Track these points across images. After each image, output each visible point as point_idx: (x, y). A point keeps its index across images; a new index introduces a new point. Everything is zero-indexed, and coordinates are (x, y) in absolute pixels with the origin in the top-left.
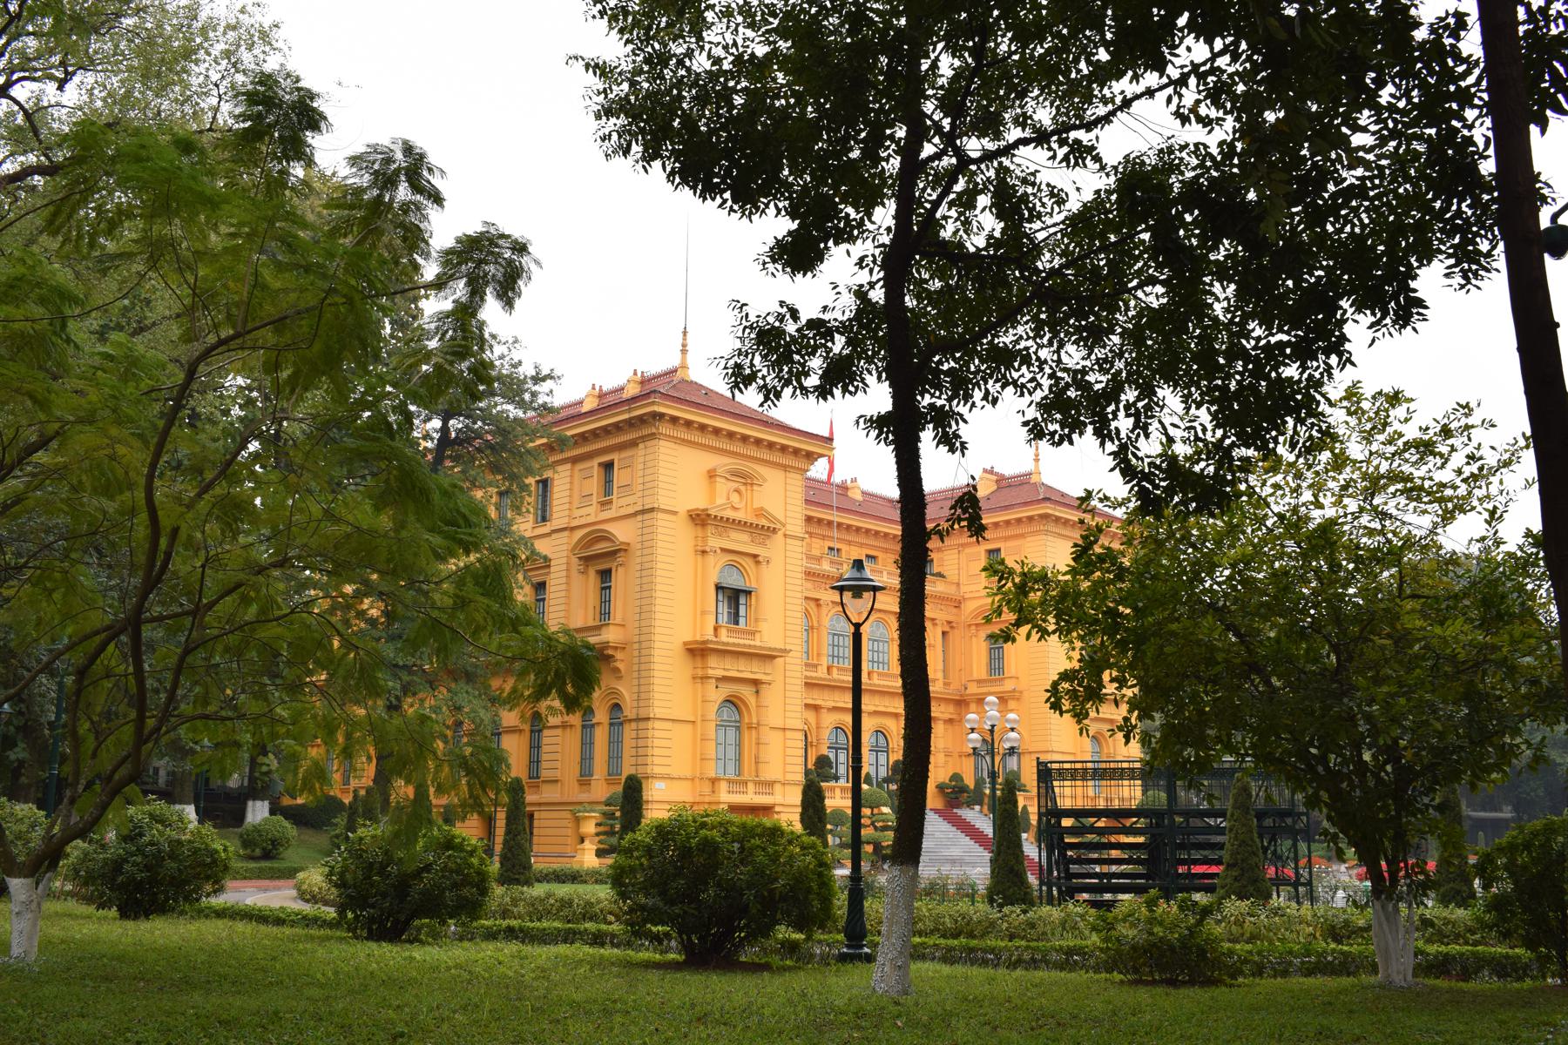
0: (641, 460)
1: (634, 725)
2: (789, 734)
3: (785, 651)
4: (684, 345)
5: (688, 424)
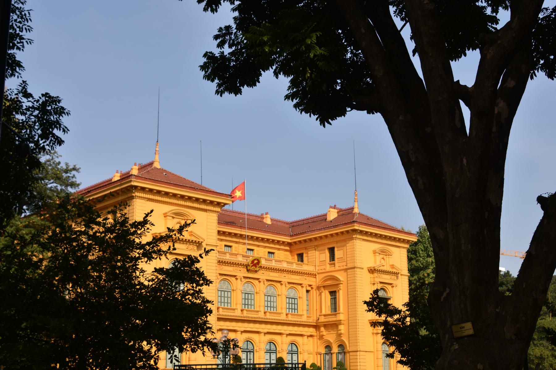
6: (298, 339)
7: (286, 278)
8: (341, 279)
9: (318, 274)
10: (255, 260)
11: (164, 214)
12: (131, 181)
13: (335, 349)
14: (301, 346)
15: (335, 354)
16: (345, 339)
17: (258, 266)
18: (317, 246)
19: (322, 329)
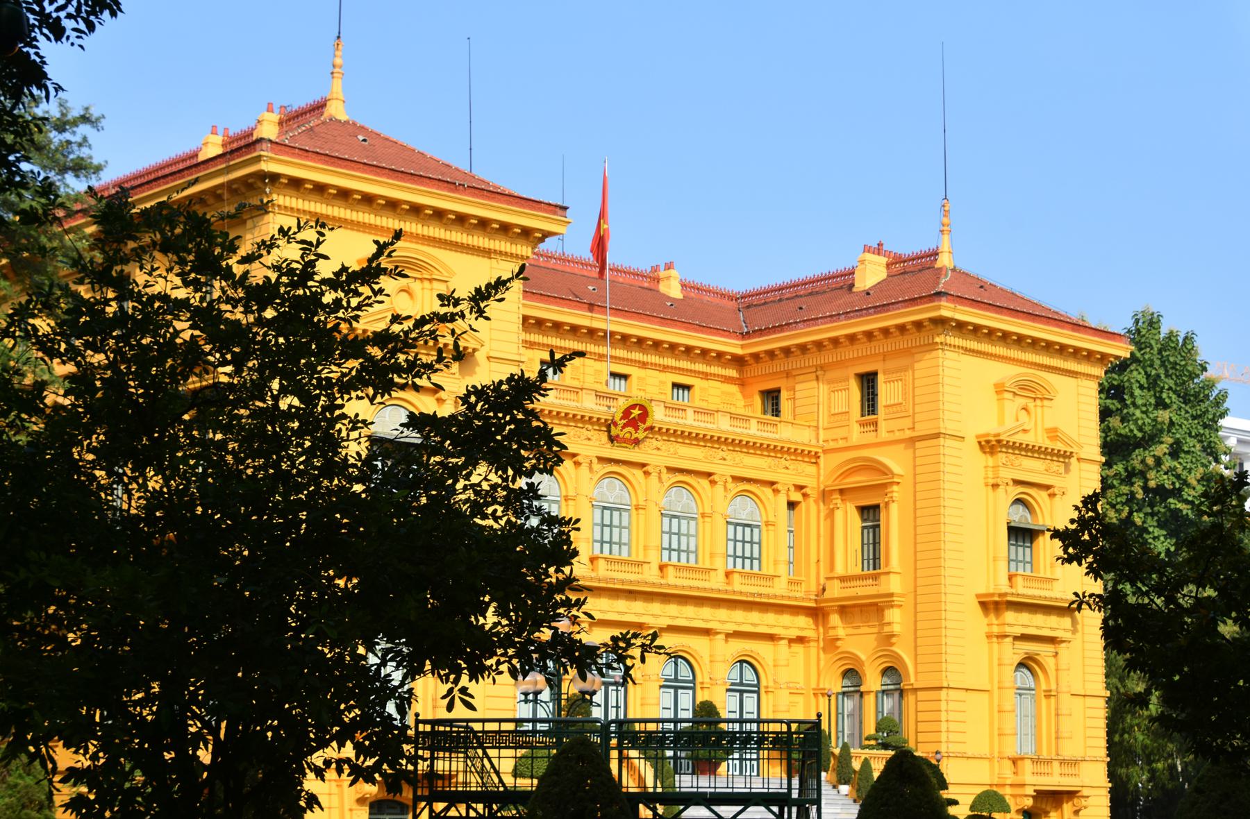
6: (762, 650)
7: (727, 464)
8: (896, 468)
9: (825, 452)
10: (633, 407)
12: (258, 159)
13: (873, 681)
14: (770, 670)
15: (872, 696)
16: (903, 651)
17: (642, 426)
18: (822, 367)
19: (835, 619)
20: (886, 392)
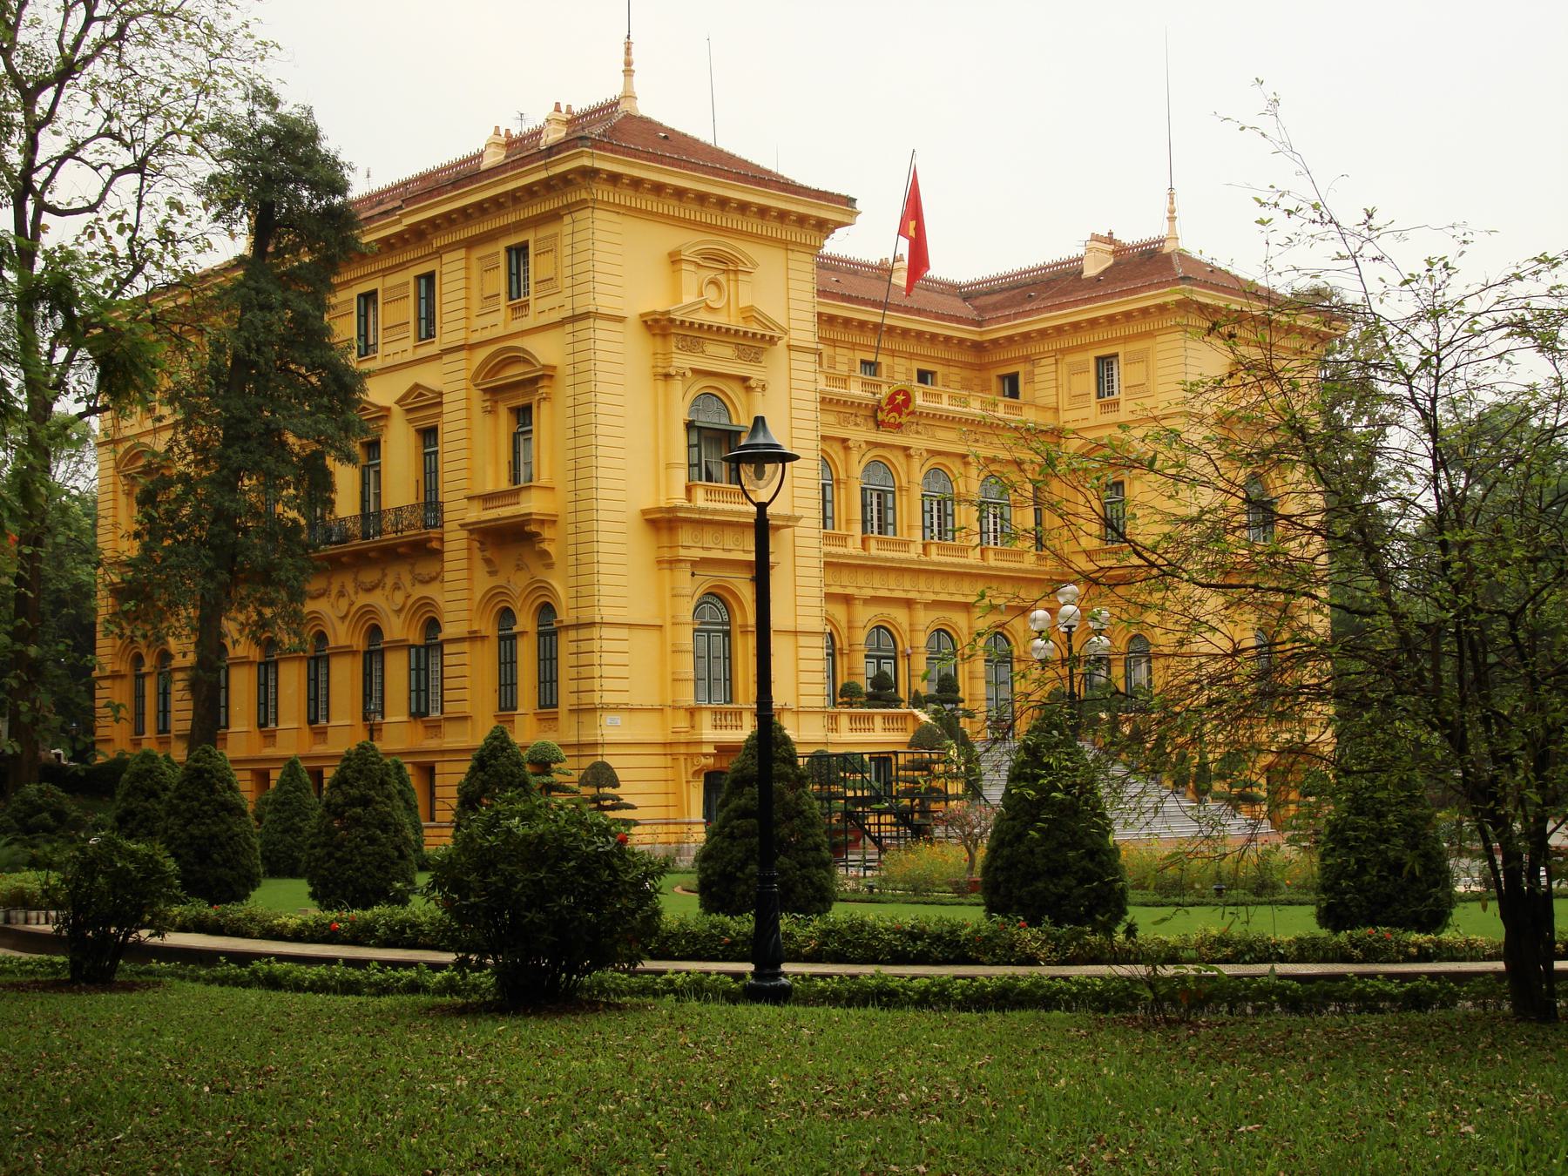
0: (568, 240)
1: (572, 634)
2: (803, 640)
3: (798, 519)
4: (628, 63)
5: (637, 183)
10: (898, 393)
11: (671, 255)
12: (580, 155)
20: (1124, 375)
